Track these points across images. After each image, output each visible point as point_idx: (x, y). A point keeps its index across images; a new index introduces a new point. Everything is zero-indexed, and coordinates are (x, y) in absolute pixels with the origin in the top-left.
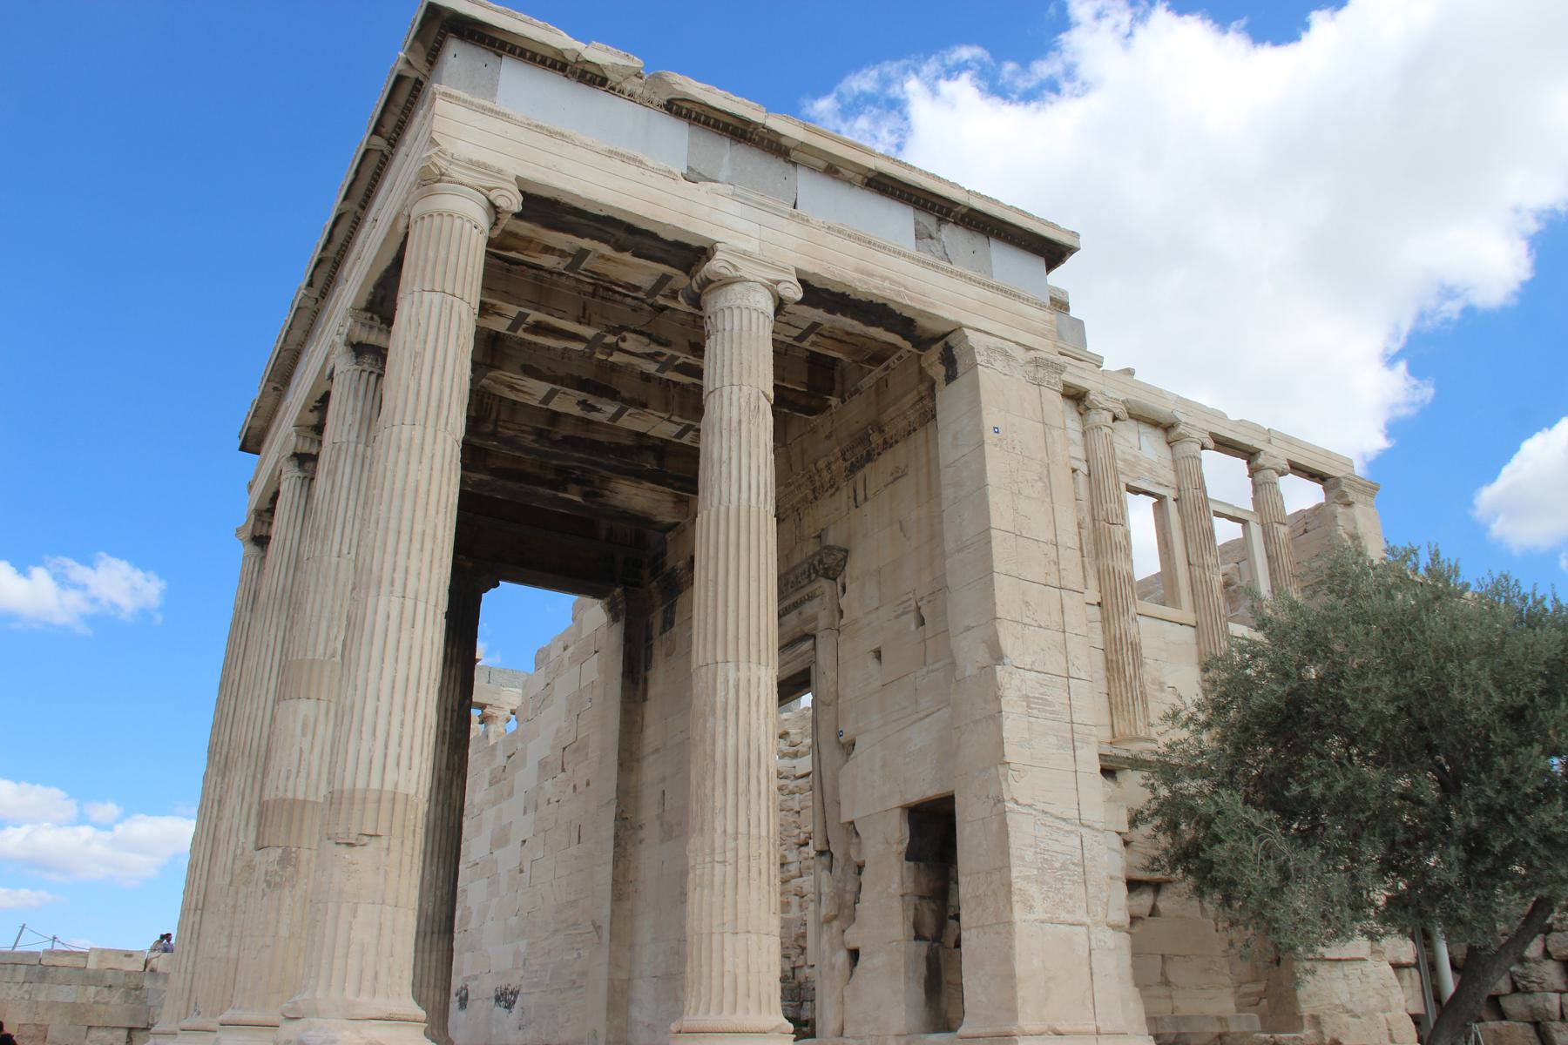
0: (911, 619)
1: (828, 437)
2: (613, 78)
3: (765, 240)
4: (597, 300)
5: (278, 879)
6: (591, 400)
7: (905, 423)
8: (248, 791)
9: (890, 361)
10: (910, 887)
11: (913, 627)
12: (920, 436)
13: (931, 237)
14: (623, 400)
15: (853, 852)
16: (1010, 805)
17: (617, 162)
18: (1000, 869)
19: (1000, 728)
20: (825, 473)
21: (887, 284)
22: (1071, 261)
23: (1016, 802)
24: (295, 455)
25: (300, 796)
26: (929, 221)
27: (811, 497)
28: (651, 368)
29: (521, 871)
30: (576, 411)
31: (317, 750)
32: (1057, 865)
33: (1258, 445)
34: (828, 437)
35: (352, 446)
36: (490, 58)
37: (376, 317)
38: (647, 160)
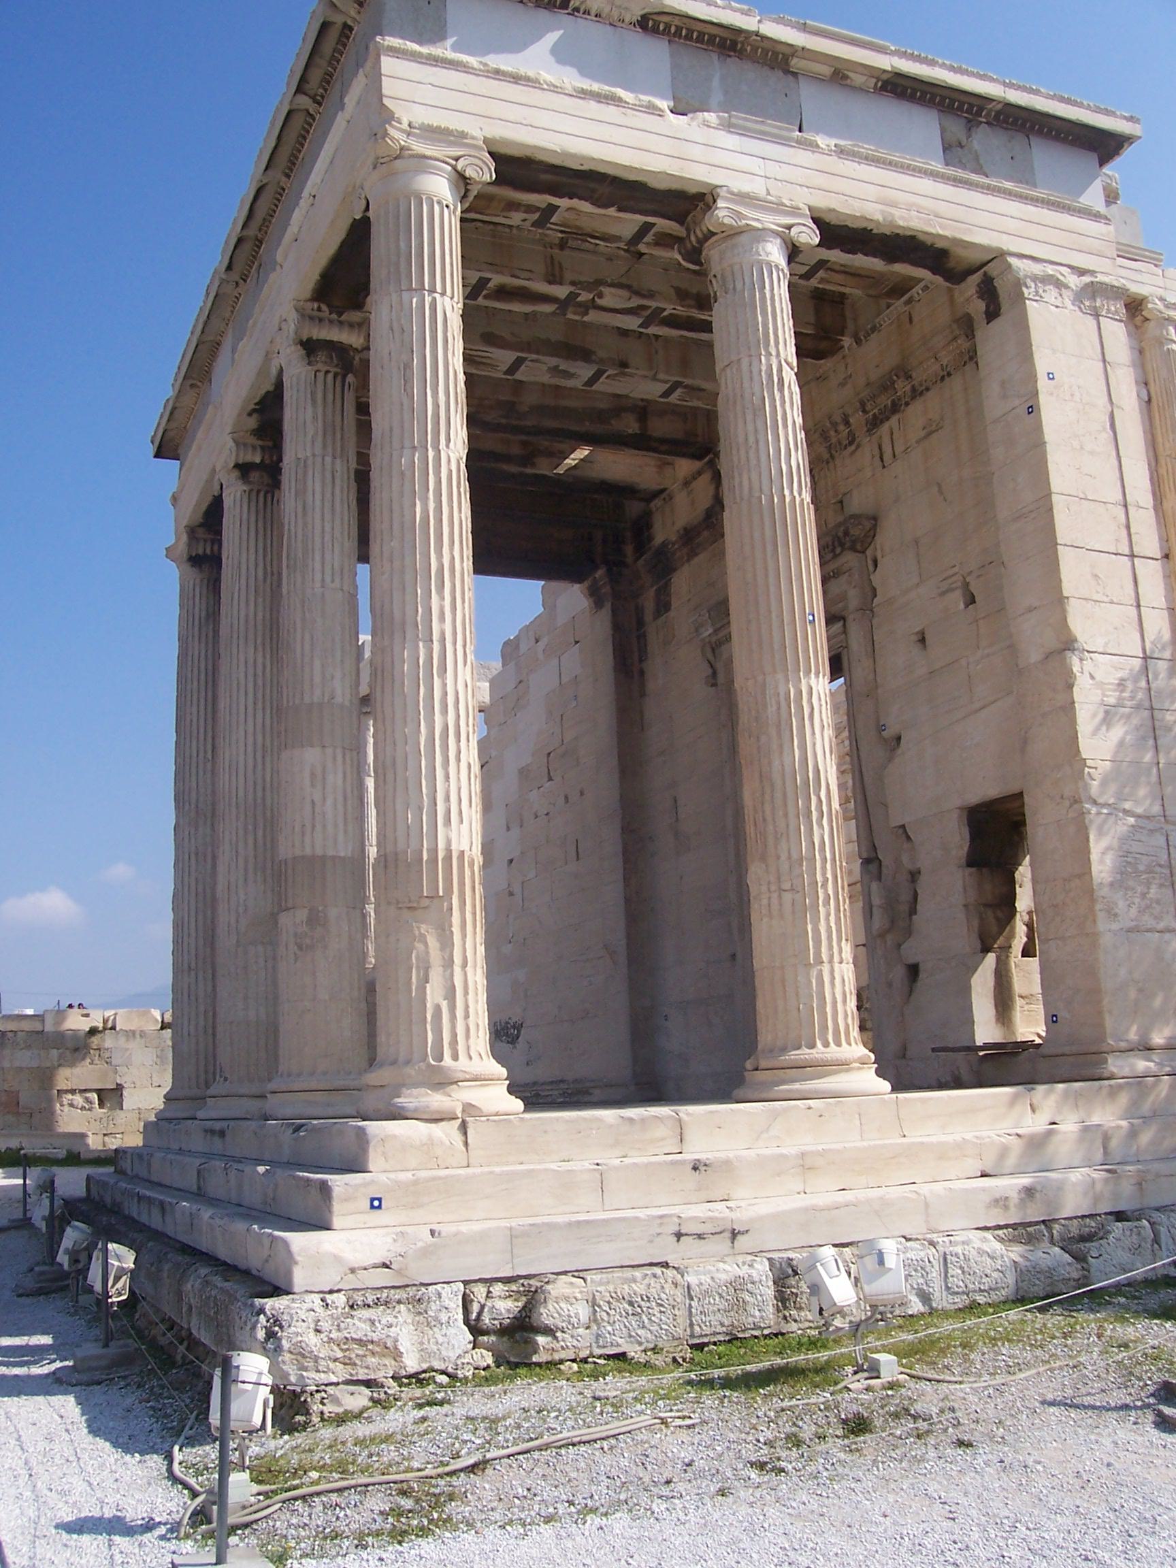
0: (956, 600)
1: (842, 384)
3: (774, 182)
4: (567, 252)
5: (308, 941)
6: (564, 365)
7: (936, 367)
8: (241, 845)
11: (962, 606)
12: (956, 382)
15: (905, 859)
18: (1080, 876)
20: (841, 427)
24: (237, 466)
25: (319, 852)
26: (956, 128)
27: (826, 456)
28: (632, 323)
29: (511, 894)
30: (546, 379)
31: (329, 802)
32: (1141, 868)
34: (842, 384)
35: (319, 459)
37: (324, 307)
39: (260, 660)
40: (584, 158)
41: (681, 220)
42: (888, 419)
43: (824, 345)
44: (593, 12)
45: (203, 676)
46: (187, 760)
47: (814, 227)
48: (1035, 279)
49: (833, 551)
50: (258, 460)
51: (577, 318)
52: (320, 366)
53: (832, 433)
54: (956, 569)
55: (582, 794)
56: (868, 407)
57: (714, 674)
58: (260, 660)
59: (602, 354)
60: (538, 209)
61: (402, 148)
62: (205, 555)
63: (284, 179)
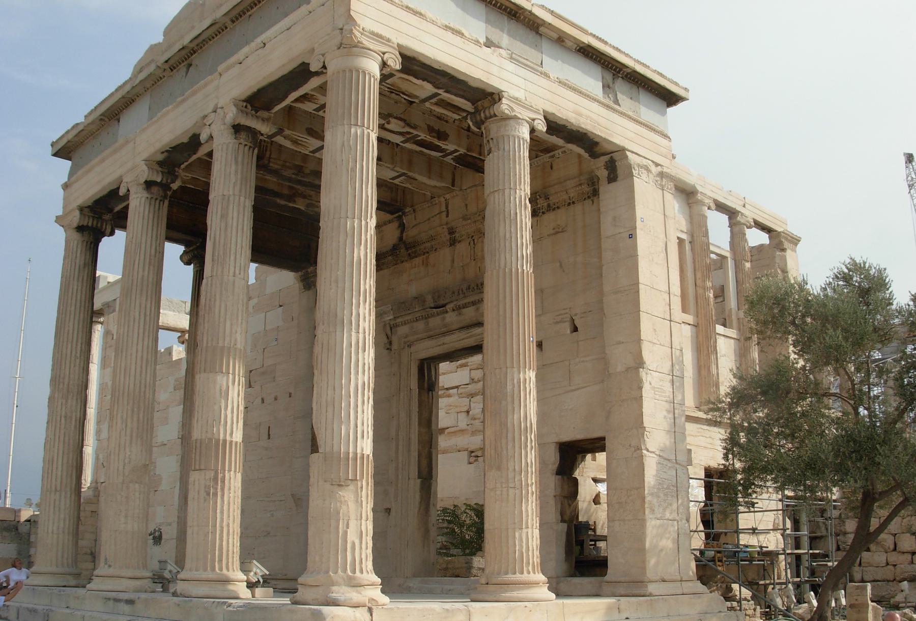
8: (129, 420)
11: (569, 332)
12: (578, 208)
16: (645, 452)
19: (641, 406)
22: (681, 105)
23: (648, 450)
24: (146, 182)
26: (609, 77)
33: (739, 208)
35: (237, 198)
37: (249, 106)
38: (466, 34)
39: (149, 306)
40: (438, 62)
41: (474, 102)
45: (78, 304)
46: (64, 356)
48: (639, 165)
50: (159, 180)
52: (242, 141)
55: (276, 399)
57: (390, 343)
58: (149, 306)
62: (87, 226)
63: (230, 22)
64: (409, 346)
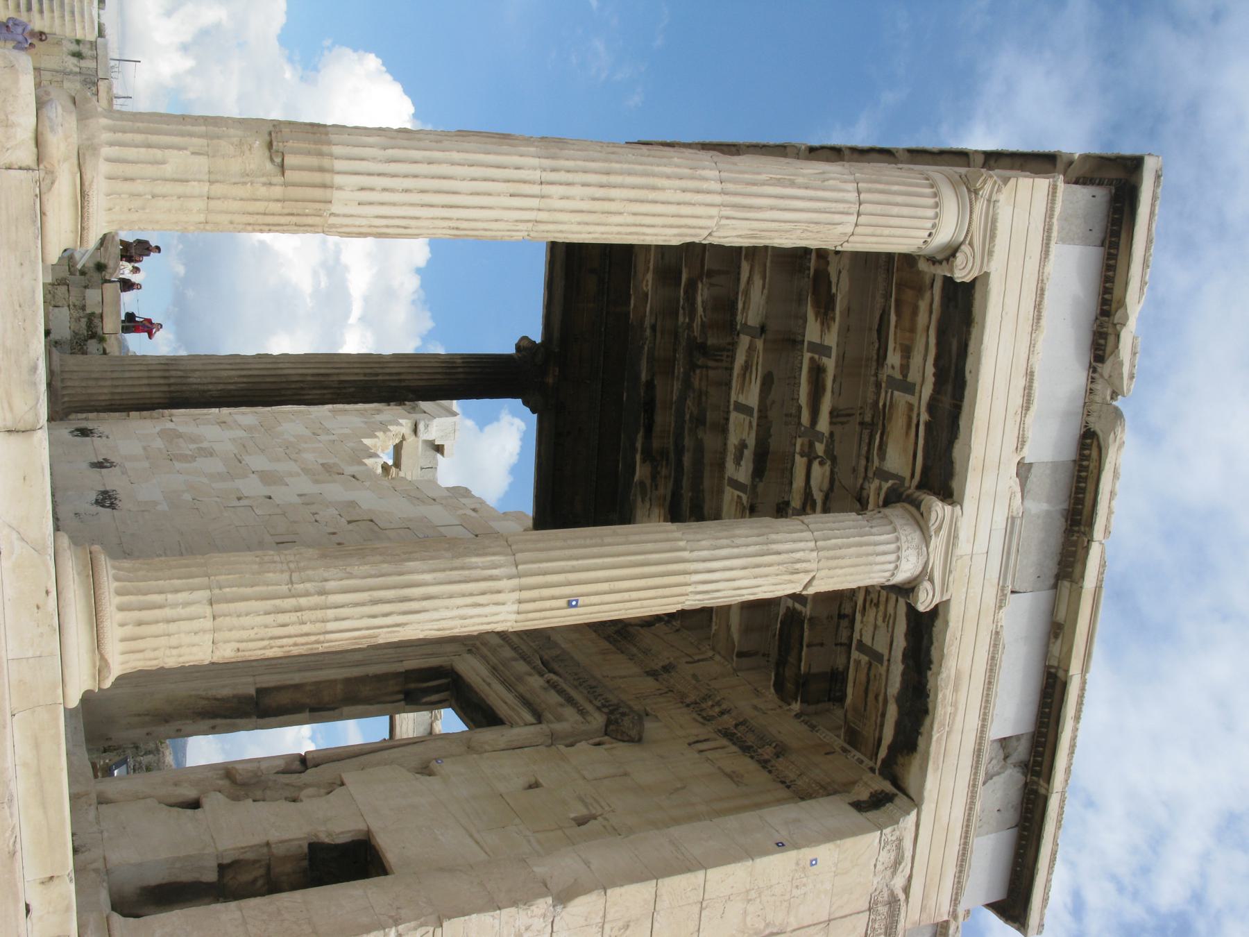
1: (755, 708)
2: (1106, 369)
4: (858, 428)
6: (748, 453)
7: (792, 776)
9: (854, 752)
10: (279, 851)
11: (572, 815)
12: (784, 793)
13: (1006, 758)
14: (754, 487)
17: (1021, 382)
20: (717, 709)
21: (949, 709)
26: (1021, 751)
27: (688, 701)
29: (239, 499)
30: (733, 440)
34: (755, 708)
36: (1098, 234)
42: (734, 744)
43: (790, 686)
44: (1093, 386)
47: (932, 606)
49: (604, 706)
51: (798, 449)
53: (710, 703)
54: (607, 808)
56: (741, 728)
59: (761, 486)
60: (905, 376)
61: (976, 192)
64: (470, 651)
